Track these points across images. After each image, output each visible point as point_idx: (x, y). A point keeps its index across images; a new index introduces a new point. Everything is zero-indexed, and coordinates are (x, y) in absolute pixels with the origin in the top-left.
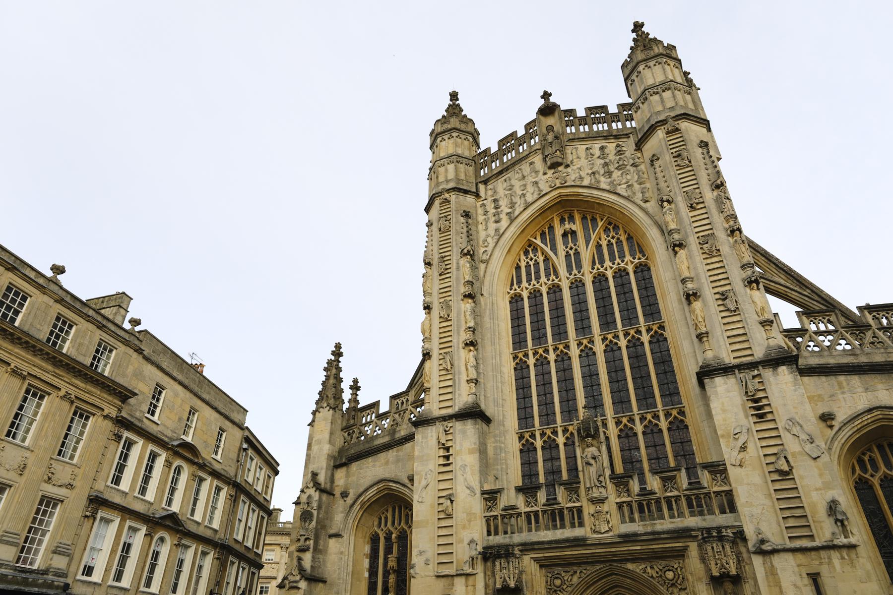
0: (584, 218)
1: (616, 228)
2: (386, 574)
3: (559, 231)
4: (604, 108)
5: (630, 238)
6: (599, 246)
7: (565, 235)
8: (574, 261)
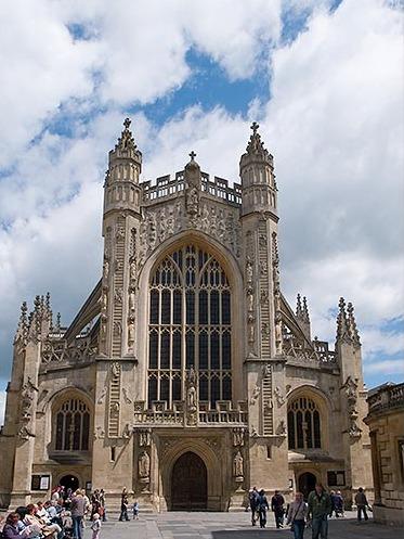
0: (200, 252)
1: (217, 265)
2: (68, 434)
3: (185, 256)
4: (225, 182)
5: (223, 273)
6: (206, 273)
7: (188, 259)
8: (191, 279)
